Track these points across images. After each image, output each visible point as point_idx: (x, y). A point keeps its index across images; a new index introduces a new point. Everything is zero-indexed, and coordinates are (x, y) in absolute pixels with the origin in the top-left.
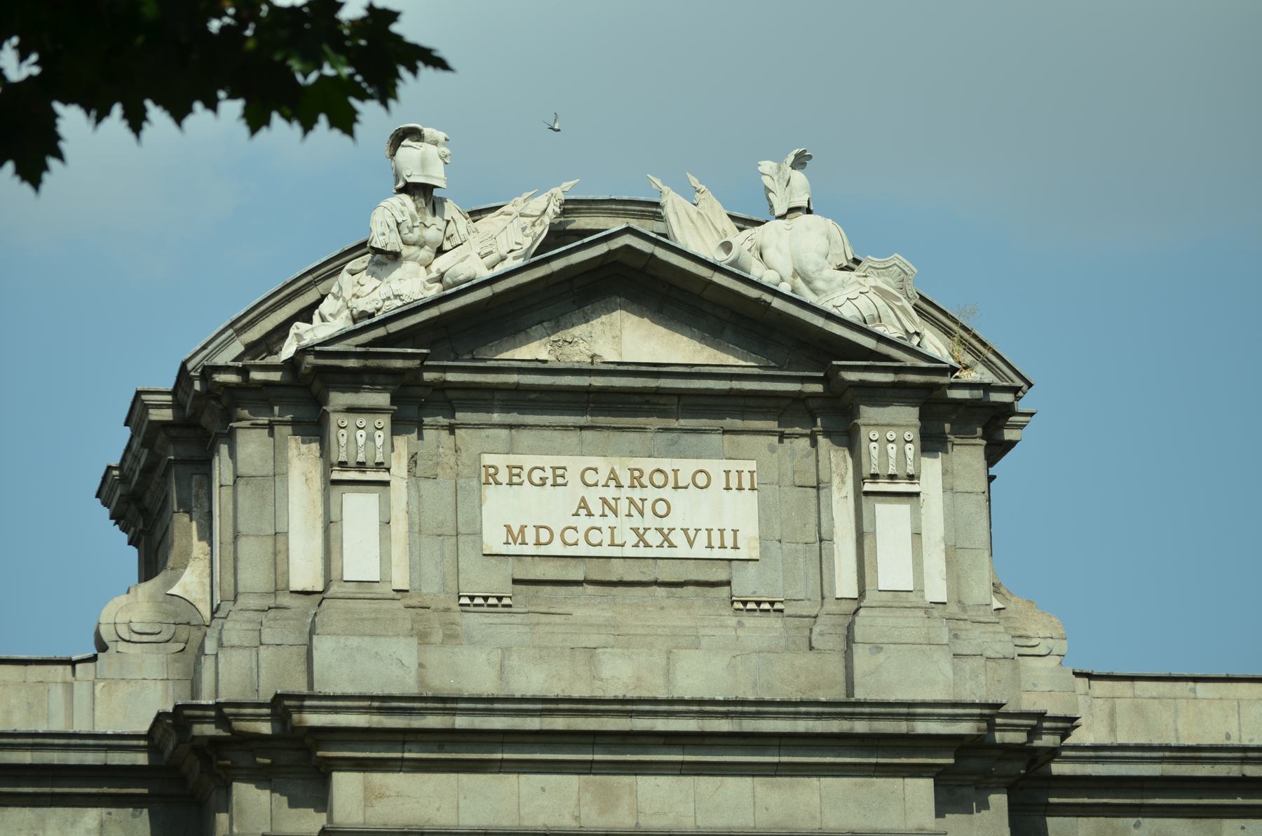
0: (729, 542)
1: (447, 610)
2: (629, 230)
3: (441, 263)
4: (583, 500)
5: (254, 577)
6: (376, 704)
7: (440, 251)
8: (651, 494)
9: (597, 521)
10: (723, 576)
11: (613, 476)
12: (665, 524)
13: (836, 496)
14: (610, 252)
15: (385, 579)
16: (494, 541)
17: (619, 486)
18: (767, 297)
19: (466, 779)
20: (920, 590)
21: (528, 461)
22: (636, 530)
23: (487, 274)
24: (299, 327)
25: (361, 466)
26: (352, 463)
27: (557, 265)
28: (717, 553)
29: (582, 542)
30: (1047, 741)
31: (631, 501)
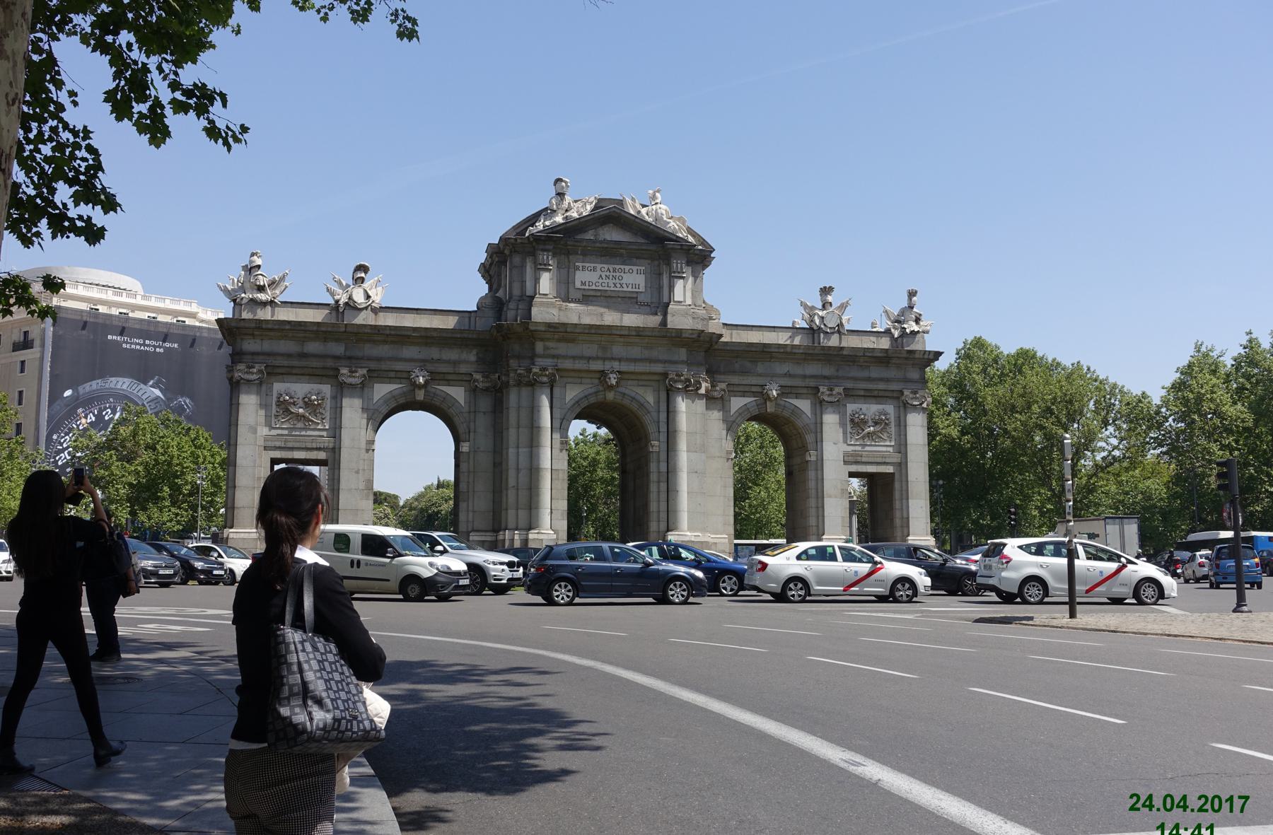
3: (568, 214)
4: (601, 276)
5: (516, 292)
7: (567, 211)
8: (618, 274)
9: (604, 281)
10: (635, 295)
11: (608, 269)
12: (622, 282)
13: (664, 277)
20: (685, 302)
21: (587, 265)
25: (545, 265)
28: (634, 290)
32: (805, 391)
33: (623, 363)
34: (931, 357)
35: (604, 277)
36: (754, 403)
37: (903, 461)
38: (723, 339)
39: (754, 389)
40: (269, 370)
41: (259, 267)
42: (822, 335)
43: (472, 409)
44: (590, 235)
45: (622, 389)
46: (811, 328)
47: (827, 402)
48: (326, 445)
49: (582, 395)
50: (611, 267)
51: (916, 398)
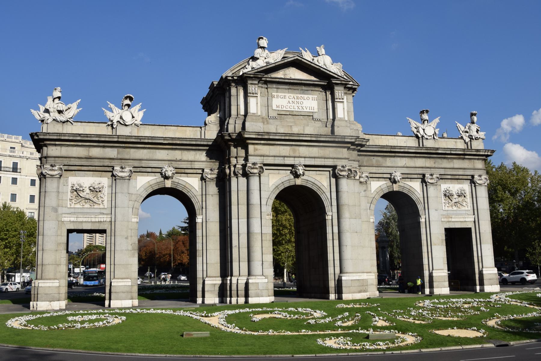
0: (313, 109)
1: (267, 119)
2: (298, 56)
6: (257, 133)
7: (265, 59)
8: (300, 100)
9: (291, 105)
10: (312, 115)
11: (294, 97)
12: (302, 105)
14: (294, 59)
15: (257, 113)
16: (274, 107)
17: (295, 99)
18: (320, 68)
19: (271, 147)
20: (344, 118)
21: (280, 94)
22: (298, 106)
23: (273, 62)
24: (243, 70)
25: (253, 94)
26: (252, 93)
27: (286, 61)
29: (289, 108)
30: (364, 143)
31: (297, 102)
32: (416, 176)
33: (306, 159)
34: (489, 154)
35: (291, 102)
36: (385, 185)
37: (477, 220)
38: (370, 143)
39: (385, 176)
40: (66, 168)
41: (59, 98)
42: (424, 140)
43: (204, 193)
44: (280, 75)
45: (304, 177)
46: (417, 137)
47: (430, 183)
48: (105, 219)
49: (281, 182)
50: (295, 96)
51: (481, 180)
